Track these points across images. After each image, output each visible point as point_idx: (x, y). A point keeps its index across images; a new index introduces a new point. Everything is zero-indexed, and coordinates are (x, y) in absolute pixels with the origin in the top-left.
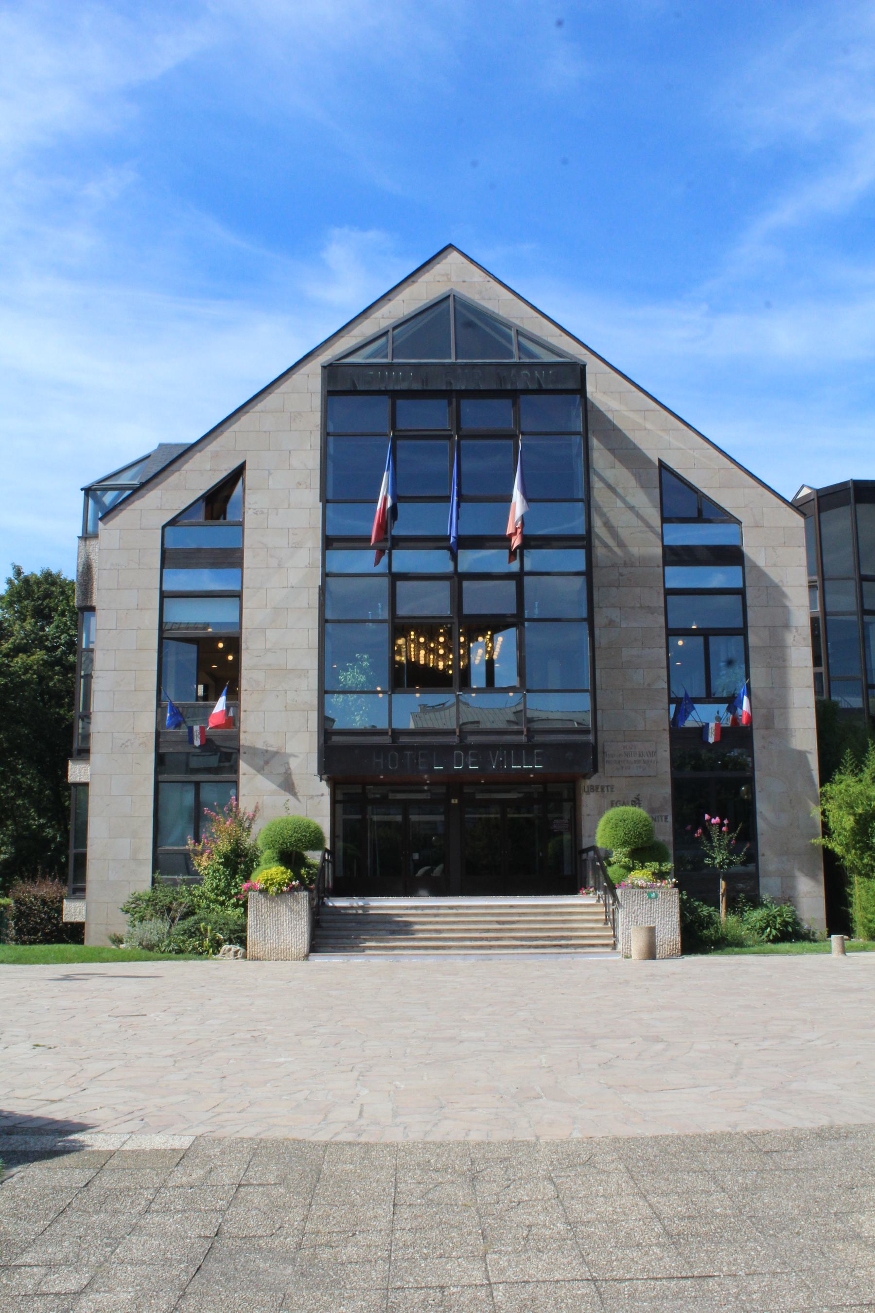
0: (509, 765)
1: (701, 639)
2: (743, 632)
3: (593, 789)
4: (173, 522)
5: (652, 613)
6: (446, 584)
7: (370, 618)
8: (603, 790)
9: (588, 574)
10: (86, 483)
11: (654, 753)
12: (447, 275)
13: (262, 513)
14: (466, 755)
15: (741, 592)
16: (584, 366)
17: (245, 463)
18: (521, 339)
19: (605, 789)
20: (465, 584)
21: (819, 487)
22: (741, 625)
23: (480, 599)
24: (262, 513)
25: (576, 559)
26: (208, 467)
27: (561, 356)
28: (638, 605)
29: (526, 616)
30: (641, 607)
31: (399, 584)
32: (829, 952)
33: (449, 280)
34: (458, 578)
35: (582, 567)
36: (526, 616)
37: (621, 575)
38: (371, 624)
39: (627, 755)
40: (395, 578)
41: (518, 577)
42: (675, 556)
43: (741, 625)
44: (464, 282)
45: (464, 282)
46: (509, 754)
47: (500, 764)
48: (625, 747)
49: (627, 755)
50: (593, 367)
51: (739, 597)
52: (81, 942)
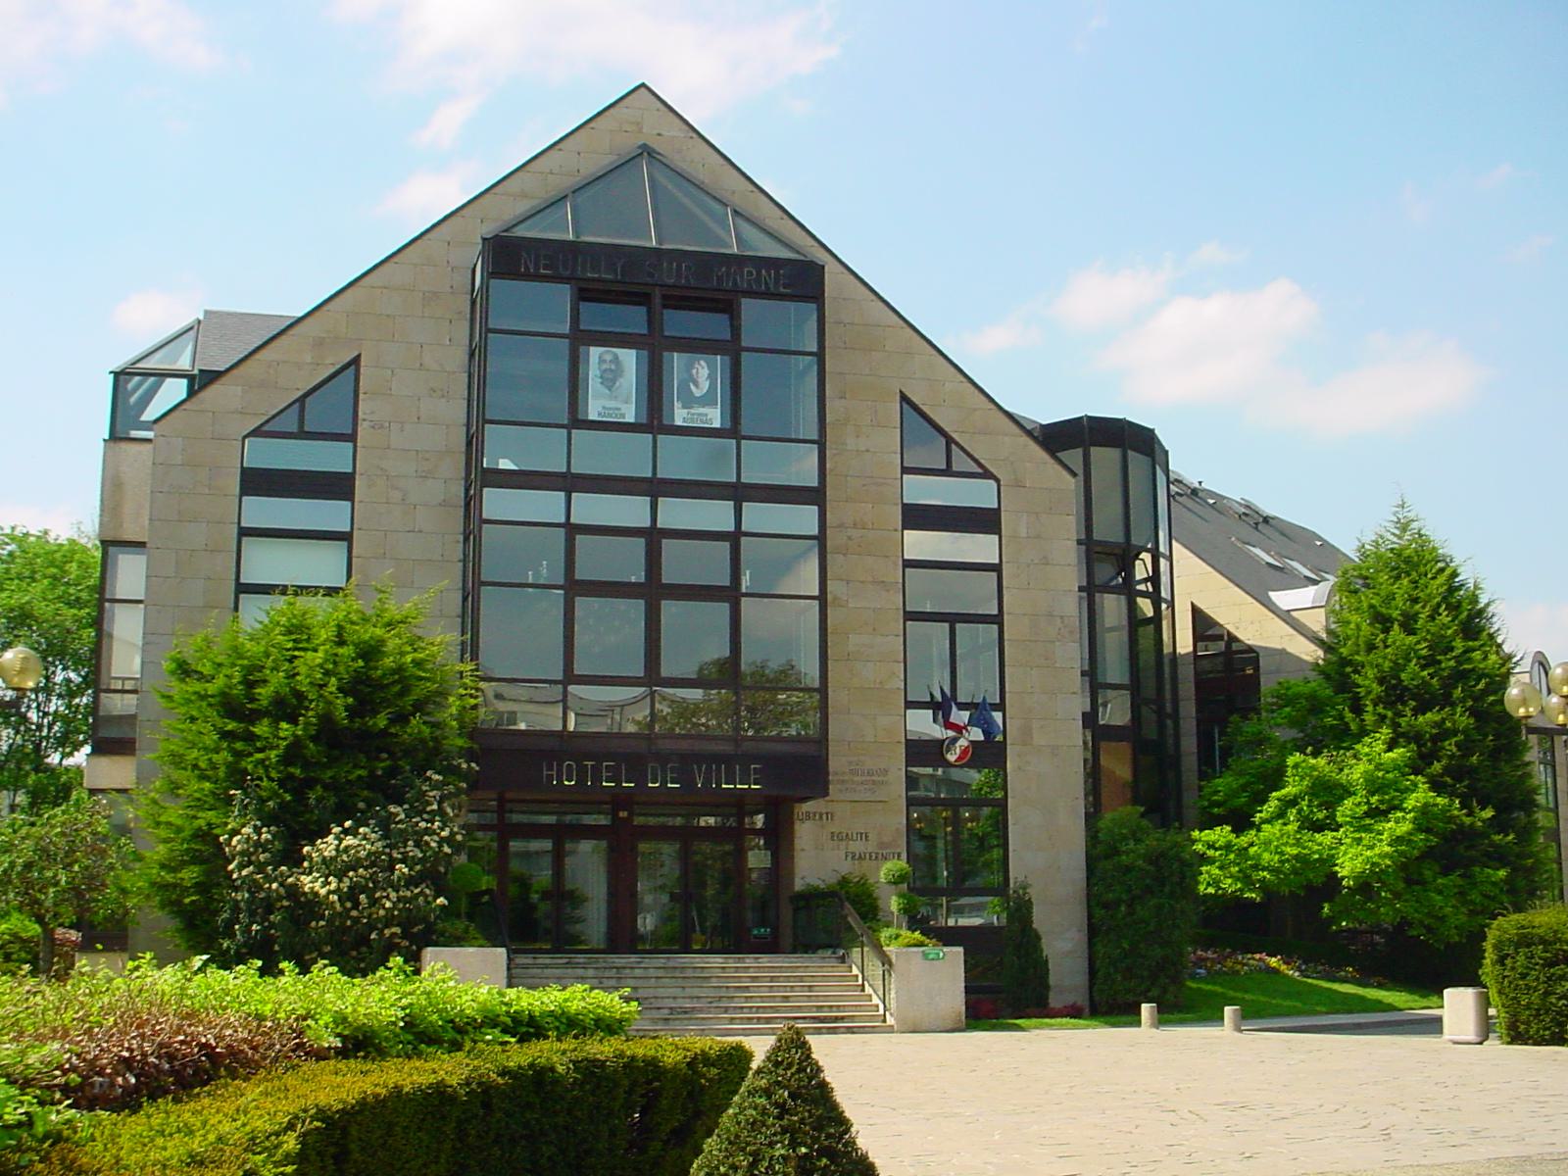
0: (719, 785)
1: (946, 625)
2: (997, 619)
3: (808, 816)
4: (257, 432)
5: (888, 591)
6: (641, 542)
7: (530, 581)
8: (821, 818)
9: (821, 538)
10: (117, 365)
11: (886, 772)
12: (638, 124)
13: (382, 427)
14: (664, 771)
15: (996, 568)
16: (823, 267)
17: (1193, 606)
18: (740, 222)
19: (824, 817)
20: (667, 544)
21: (1044, 423)
22: (995, 612)
23: (679, 564)
24: (382, 427)
25: (804, 519)
26: (308, 359)
27: (798, 252)
28: (870, 579)
29: (744, 590)
30: (874, 582)
31: (580, 539)
32: (1138, 1024)
33: (640, 131)
34: (653, 537)
35: (815, 531)
36: (744, 590)
37: (849, 538)
38: (530, 590)
39: (853, 772)
40: (572, 530)
41: (735, 538)
42: (919, 517)
43: (995, 612)
44: (659, 135)
45: (659, 135)
46: (719, 770)
47: (707, 781)
48: (850, 763)
49: (853, 772)
50: (831, 272)
51: (994, 575)
52: (1440, 1031)
